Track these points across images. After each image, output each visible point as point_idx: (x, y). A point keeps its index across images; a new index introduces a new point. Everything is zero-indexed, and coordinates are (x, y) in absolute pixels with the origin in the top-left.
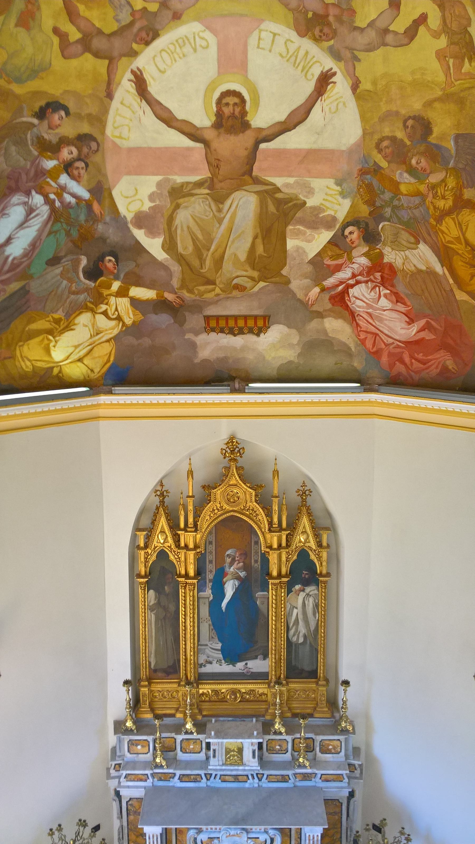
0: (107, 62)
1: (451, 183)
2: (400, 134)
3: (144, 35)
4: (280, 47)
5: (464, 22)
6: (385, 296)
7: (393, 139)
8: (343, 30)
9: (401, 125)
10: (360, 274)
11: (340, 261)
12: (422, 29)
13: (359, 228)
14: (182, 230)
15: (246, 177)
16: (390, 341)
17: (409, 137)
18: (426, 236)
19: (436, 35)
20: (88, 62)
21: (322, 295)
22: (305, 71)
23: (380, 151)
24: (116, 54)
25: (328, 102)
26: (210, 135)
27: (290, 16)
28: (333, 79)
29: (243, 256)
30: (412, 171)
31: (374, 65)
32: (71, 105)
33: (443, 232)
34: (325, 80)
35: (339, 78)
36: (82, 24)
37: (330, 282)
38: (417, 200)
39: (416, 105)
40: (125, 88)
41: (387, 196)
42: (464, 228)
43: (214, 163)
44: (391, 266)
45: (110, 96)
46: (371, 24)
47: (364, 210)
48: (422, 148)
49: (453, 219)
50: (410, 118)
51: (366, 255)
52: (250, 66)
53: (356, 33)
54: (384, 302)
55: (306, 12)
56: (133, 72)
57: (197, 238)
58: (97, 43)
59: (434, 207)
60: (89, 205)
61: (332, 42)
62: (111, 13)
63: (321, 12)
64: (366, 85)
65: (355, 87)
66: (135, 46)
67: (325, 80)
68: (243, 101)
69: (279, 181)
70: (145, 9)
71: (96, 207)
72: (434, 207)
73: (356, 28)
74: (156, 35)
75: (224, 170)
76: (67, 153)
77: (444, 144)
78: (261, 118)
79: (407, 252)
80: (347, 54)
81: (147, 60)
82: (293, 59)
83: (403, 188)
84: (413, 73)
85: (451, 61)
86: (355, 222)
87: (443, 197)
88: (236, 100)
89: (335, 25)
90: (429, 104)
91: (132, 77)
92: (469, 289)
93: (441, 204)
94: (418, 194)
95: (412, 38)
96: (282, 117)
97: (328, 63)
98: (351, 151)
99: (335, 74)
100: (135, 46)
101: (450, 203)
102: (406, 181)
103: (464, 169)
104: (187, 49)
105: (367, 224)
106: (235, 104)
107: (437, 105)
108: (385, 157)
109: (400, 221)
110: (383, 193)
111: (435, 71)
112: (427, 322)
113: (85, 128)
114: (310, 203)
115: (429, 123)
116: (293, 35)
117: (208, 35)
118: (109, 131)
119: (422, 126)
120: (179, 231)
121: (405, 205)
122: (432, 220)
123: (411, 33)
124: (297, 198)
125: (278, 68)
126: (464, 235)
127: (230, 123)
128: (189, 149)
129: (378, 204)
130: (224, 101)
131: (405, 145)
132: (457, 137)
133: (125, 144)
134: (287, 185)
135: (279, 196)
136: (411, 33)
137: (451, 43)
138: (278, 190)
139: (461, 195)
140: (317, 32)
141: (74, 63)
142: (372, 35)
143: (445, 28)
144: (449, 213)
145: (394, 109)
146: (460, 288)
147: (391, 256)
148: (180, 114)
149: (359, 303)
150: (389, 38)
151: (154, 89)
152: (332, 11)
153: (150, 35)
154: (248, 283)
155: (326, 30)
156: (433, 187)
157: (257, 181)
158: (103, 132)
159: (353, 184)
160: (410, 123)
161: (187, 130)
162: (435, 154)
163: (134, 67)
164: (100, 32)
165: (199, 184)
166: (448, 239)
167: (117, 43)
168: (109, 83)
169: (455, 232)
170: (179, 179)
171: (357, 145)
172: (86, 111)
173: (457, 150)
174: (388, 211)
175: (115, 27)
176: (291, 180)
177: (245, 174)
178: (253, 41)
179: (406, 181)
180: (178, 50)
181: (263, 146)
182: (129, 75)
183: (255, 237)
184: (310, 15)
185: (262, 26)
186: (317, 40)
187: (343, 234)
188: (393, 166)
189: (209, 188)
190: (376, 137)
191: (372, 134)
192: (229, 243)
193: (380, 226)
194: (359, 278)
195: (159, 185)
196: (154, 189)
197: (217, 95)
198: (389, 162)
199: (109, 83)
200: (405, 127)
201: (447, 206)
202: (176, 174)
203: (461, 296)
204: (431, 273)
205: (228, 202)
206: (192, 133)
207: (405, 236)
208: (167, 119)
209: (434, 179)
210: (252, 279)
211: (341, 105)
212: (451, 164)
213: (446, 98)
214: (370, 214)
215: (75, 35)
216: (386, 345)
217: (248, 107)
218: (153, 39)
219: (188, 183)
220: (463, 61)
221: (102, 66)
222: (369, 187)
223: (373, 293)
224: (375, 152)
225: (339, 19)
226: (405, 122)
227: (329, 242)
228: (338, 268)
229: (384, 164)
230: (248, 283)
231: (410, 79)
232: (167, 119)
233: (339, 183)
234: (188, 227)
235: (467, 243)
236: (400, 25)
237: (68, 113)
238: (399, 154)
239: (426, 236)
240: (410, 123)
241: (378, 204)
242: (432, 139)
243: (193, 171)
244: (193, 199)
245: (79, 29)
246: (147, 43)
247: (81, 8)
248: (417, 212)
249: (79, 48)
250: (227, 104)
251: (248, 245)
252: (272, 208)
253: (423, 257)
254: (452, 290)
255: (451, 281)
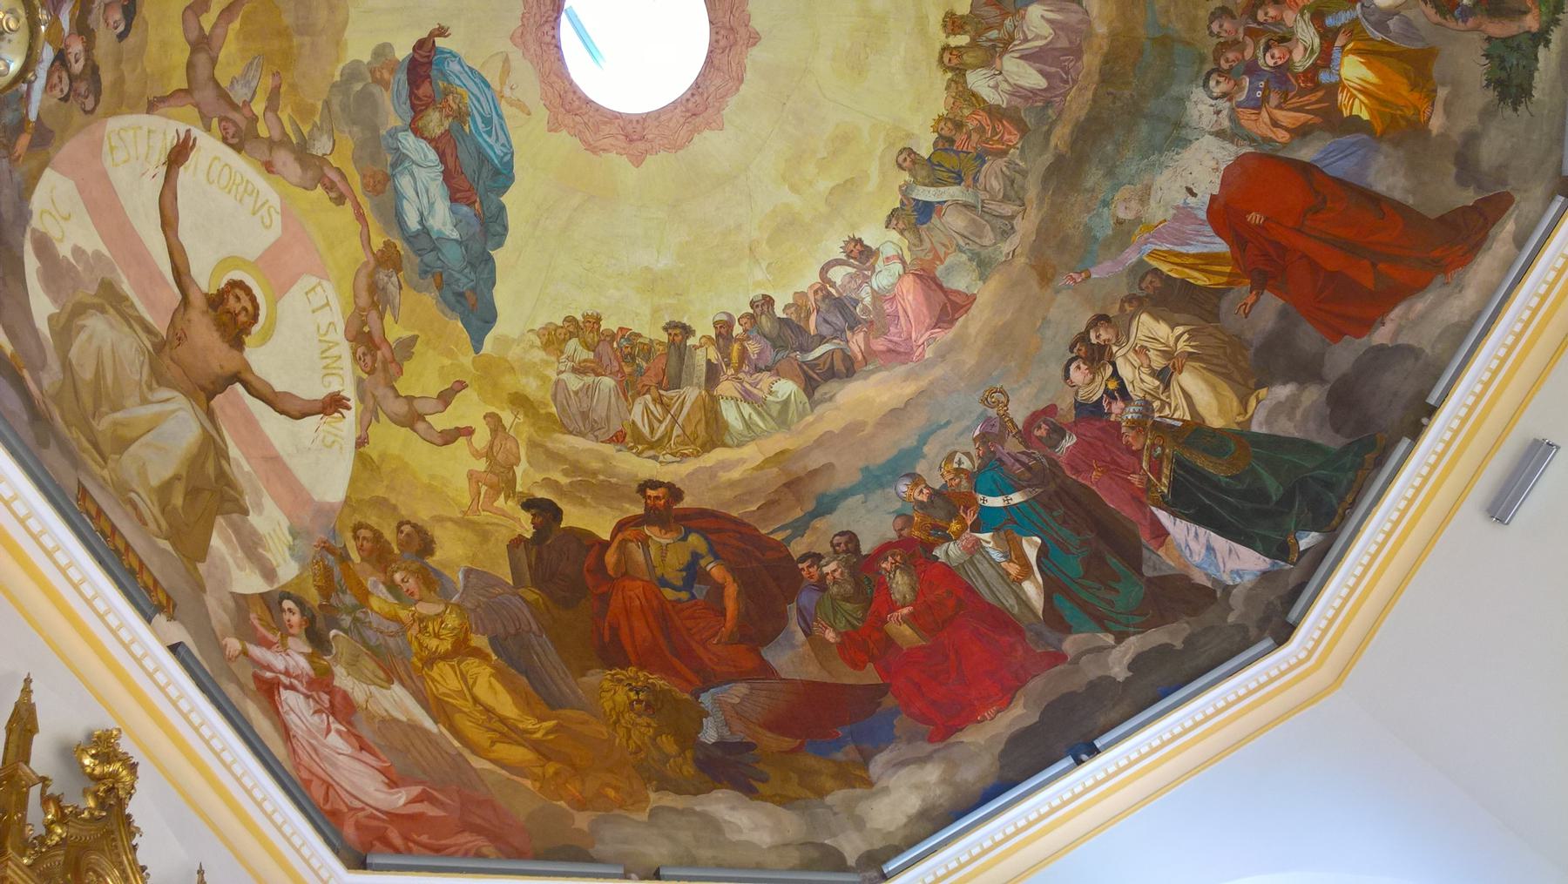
0: (185, 86)
1: (452, 621)
2: (389, 534)
3: (231, 130)
4: (324, 318)
5: (512, 459)
6: (339, 732)
7: (378, 536)
8: (380, 375)
9: (394, 524)
10: (296, 677)
11: (270, 636)
12: (462, 440)
13: (303, 614)
14: (91, 337)
15: (202, 396)
16: (360, 805)
17: (400, 545)
18: (405, 677)
19: (477, 455)
20: (181, 54)
21: (242, 658)
22: (328, 372)
23: (356, 538)
24: (198, 96)
25: (326, 427)
26: (198, 301)
27: (350, 309)
28: (344, 411)
29: (155, 482)
30: (392, 587)
31: (391, 439)
32: (132, 39)
33: (433, 680)
34: (334, 404)
35: (350, 415)
36: (219, 31)
37: (257, 652)
38: (393, 627)
39: (423, 513)
40: (164, 129)
41: (349, 599)
42: (470, 682)
43: (178, 334)
44: (346, 696)
45: (152, 107)
46: (410, 399)
47: (314, 598)
48: (415, 566)
49: (452, 667)
50: (408, 523)
51: (309, 657)
52: (287, 299)
53: (391, 394)
54: (334, 740)
55: (364, 323)
56: (188, 131)
57: (104, 377)
58: (202, 58)
59: (420, 644)
60: (24, 120)
61: (365, 376)
62: (237, 71)
63: (377, 340)
64: (371, 450)
65: (361, 442)
66: (215, 122)
67: (334, 404)
68: (255, 318)
69: (234, 451)
70: (255, 119)
71: (24, 141)
72: (420, 644)
73: (393, 388)
74: (238, 148)
75: (182, 352)
76: (76, 47)
77: (447, 572)
78: (262, 358)
79: (372, 688)
80: (371, 403)
81: (209, 147)
82: (325, 346)
83: (375, 603)
84: (433, 477)
85: (484, 489)
86: (300, 603)
87: (437, 636)
88: (250, 308)
89: (378, 365)
90: (440, 520)
91: (182, 136)
92: (492, 755)
93: (433, 643)
94: (396, 619)
95: (446, 443)
96: (279, 387)
97: (349, 392)
98: (322, 511)
99: (348, 408)
100: (215, 122)
101: (446, 646)
102: (381, 599)
103: (474, 610)
104: (249, 200)
105: (314, 617)
106: (245, 309)
107: (449, 524)
108: (360, 549)
109: (365, 643)
110: (344, 592)
111: (461, 489)
112: (424, 791)
113: (107, 78)
114: (253, 518)
115: (432, 541)
116: (341, 327)
117: (277, 219)
118: (113, 124)
119: (421, 543)
120: (83, 336)
121: (374, 625)
122: (415, 660)
123: (449, 437)
124: (241, 494)
125: (303, 341)
126: (470, 690)
127: (225, 318)
128: (161, 275)
129: (333, 601)
130: (238, 291)
131: (391, 552)
132: (468, 572)
133: (108, 163)
134: (239, 466)
135: (226, 466)
136: (449, 437)
137: (490, 470)
138: (227, 459)
139: (466, 639)
140: (361, 350)
141: (178, 32)
142: (401, 408)
143: (489, 454)
144: (445, 657)
145: (393, 501)
146: (474, 752)
147: (343, 679)
148: (185, 235)
149: (293, 716)
150: (420, 426)
151: (184, 175)
152: (385, 349)
153: (239, 139)
154: (152, 526)
155: (368, 359)
156: (422, 619)
157: (210, 414)
158: (115, 111)
159: (311, 552)
160: (407, 529)
161: (179, 262)
162: (432, 580)
163: (197, 132)
164: (214, 61)
165: (148, 330)
166: (442, 690)
167: (207, 95)
168: (163, 100)
169: (453, 683)
170: (126, 287)
171: (331, 505)
172: (126, 68)
173: (465, 586)
174: (346, 620)
175: (225, 84)
176: (247, 468)
177: (206, 391)
178: (308, 281)
179: (381, 599)
180: (241, 188)
181: (239, 387)
182: (183, 129)
183: (177, 477)
184: (366, 329)
185: (325, 283)
186: (356, 359)
187: (280, 603)
188: (367, 566)
189: (154, 345)
190: (358, 518)
191: (354, 510)
192: (142, 440)
193: (333, 633)
194: (296, 682)
195: (98, 255)
196: (89, 251)
197: (237, 275)
198: (363, 559)
199: (163, 100)
200: (399, 530)
201: (442, 649)
202: (128, 277)
203: (478, 763)
204: (414, 727)
205: (165, 393)
206: (181, 273)
207: (369, 665)
208: (169, 223)
209: (424, 609)
210: (159, 526)
211: (336, 446)
212: (455, 599)
213: (464, 523)
214: (320, 606)
215: (208, 21)
216: (351, 809)
217: (255, 329)
218: (232, 146)
219: (132, 305)
220: (498, 494)
221: (179, 81)
222: (327, 573)
223: (316, 717)
224: (349, 535)
225: (385, 362)
226: (401, 524)
227: (262, 595)
228: (268, 645)
229: (355, 556)
230: (152, 526)
231: (425, 480)
232: (169, 223)
233: (294, 534)
234: (100, 349)
235: (476, 700)
236: (441, 422)
237: (122, 36)
238: (379, 554)
239: (405, 677)
240: (407, 529)
241: (333, 601)
242: (431, 561)
243: (151, 306)
244: (126, 329)
245: (215, 26)
246: (225, 140)
247: (236, 25)
248: (391, 642)
249: (194, 35)
250: (238, 299)
251: (167, 474)
252: (210, 468)
253: (397, 702)
254: (461, 755)
255: (456, 744)
